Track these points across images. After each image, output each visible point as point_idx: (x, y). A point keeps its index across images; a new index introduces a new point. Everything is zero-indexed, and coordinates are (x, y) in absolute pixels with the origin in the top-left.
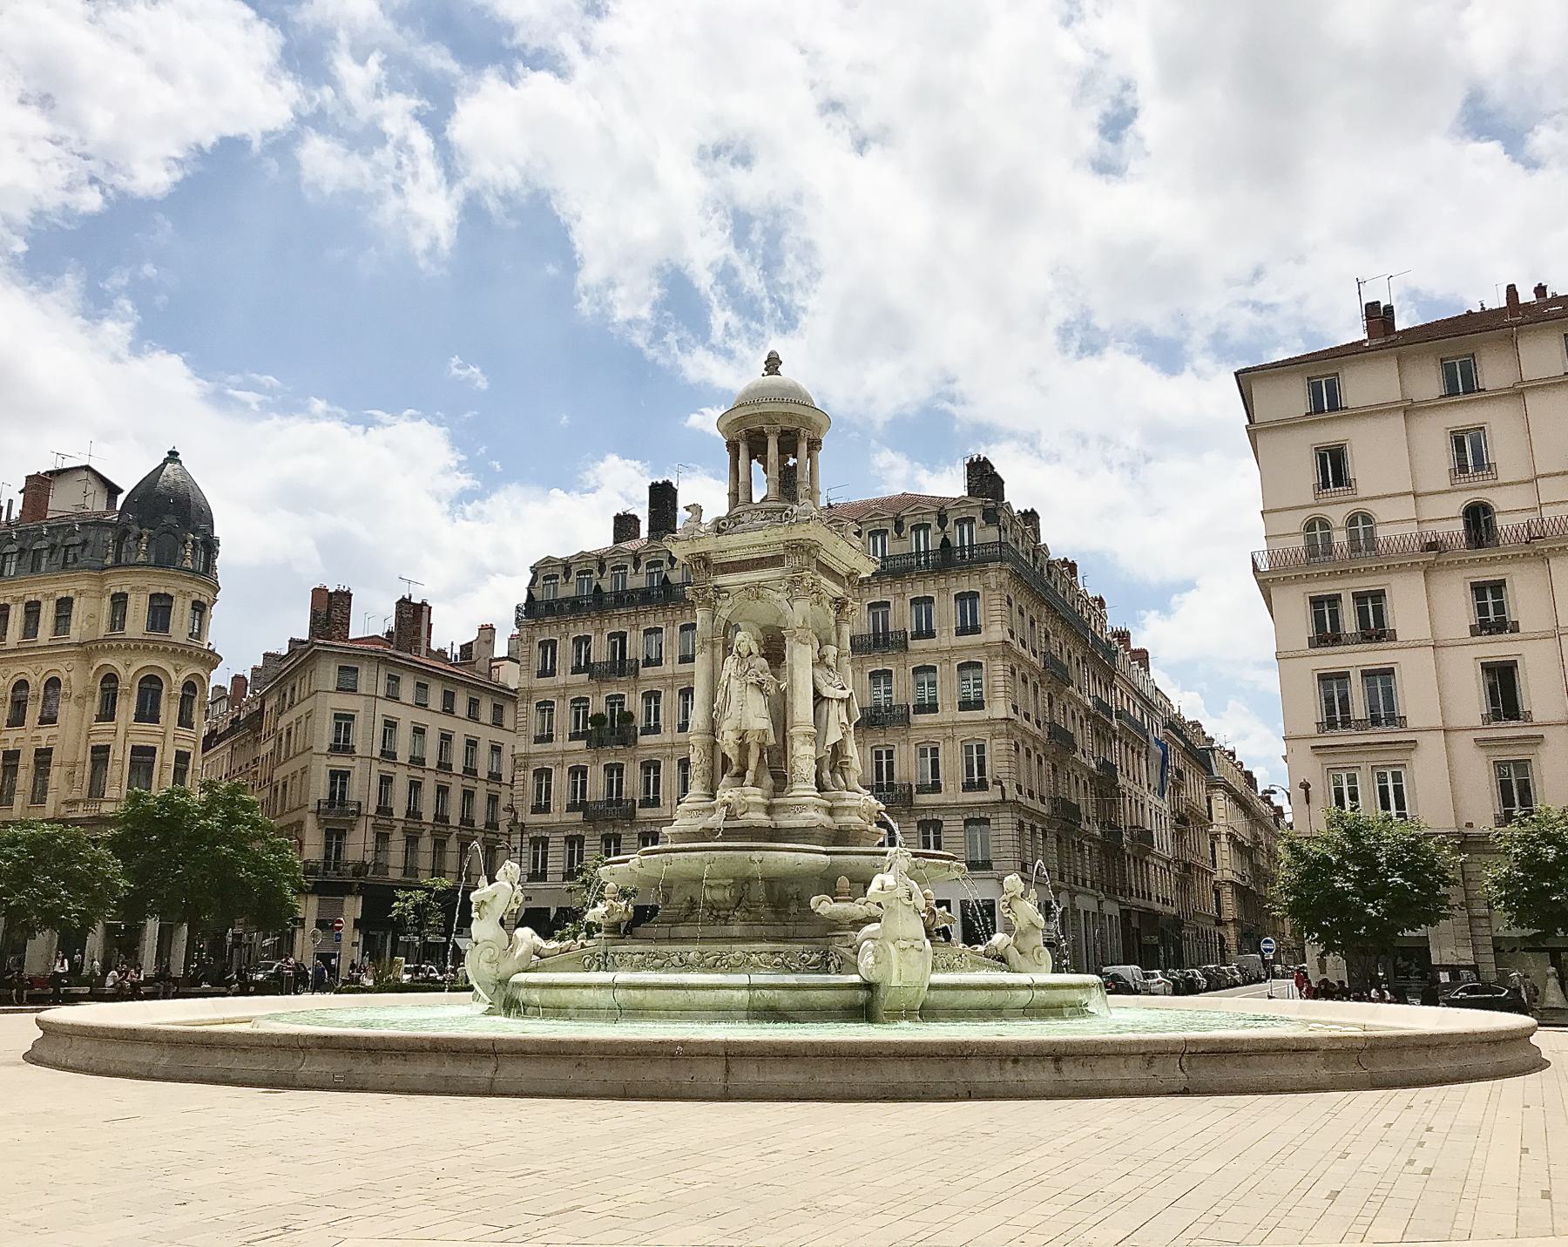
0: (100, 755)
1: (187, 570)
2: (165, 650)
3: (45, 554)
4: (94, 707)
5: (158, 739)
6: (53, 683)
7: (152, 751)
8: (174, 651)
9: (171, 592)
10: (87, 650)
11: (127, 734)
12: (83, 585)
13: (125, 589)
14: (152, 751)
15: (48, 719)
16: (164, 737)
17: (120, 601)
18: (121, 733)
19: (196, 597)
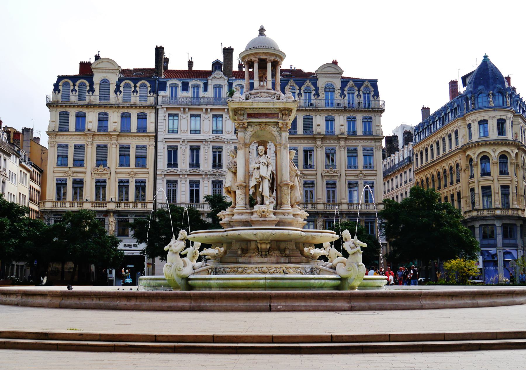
0: (472, 190)
1: (492, 107)
2: (486, 144)
3: (450, 114)
4: (469, 173)
5: (491, 182)
6: (458, 165)
7: (490, 187)
8: (490, 143)
9: (486, 118)
10: (464, 149)
11: (478, 182)
12: (459, 123)
13: (470, 122)
14: (490, 187)
15: (458, 181)
16: (493, 180)
17: (469, 126)
18: (476, 182)
19: (498, 117)
